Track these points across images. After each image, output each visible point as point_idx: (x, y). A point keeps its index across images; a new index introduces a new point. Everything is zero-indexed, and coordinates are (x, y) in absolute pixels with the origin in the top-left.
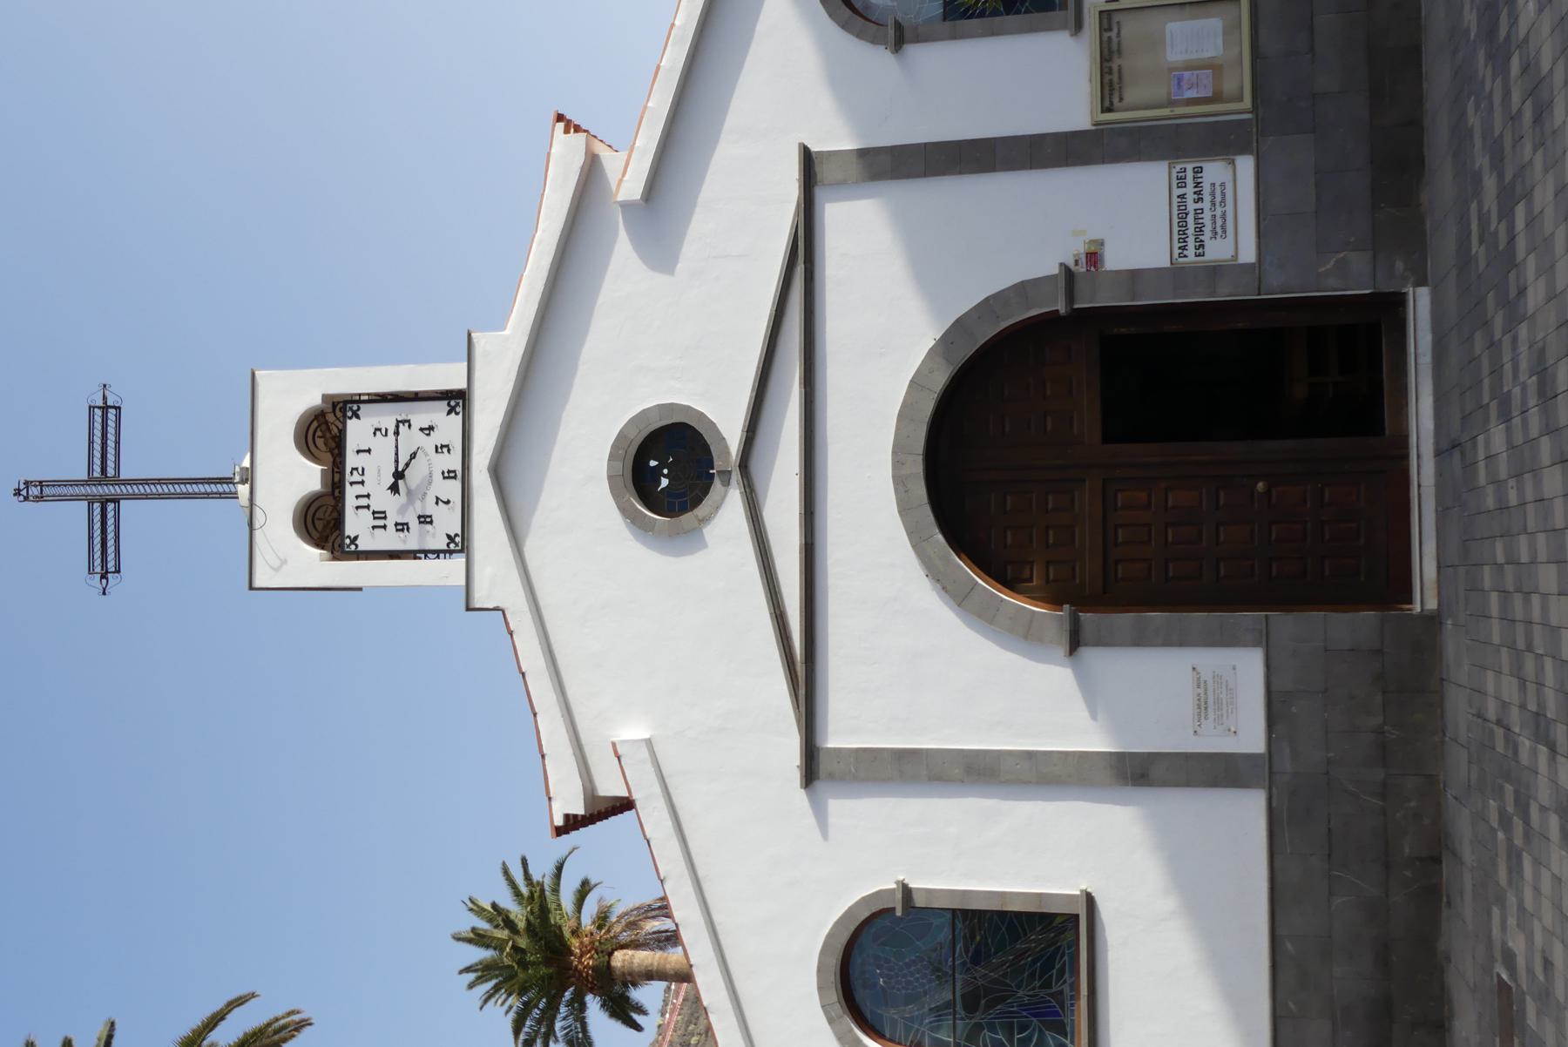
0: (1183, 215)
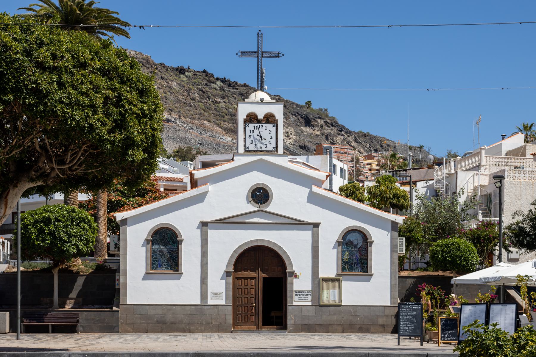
0: (303, 292)
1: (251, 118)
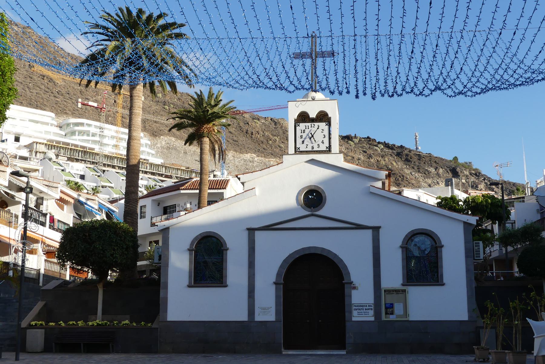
0: (362, 306)
1: (303, 117)
